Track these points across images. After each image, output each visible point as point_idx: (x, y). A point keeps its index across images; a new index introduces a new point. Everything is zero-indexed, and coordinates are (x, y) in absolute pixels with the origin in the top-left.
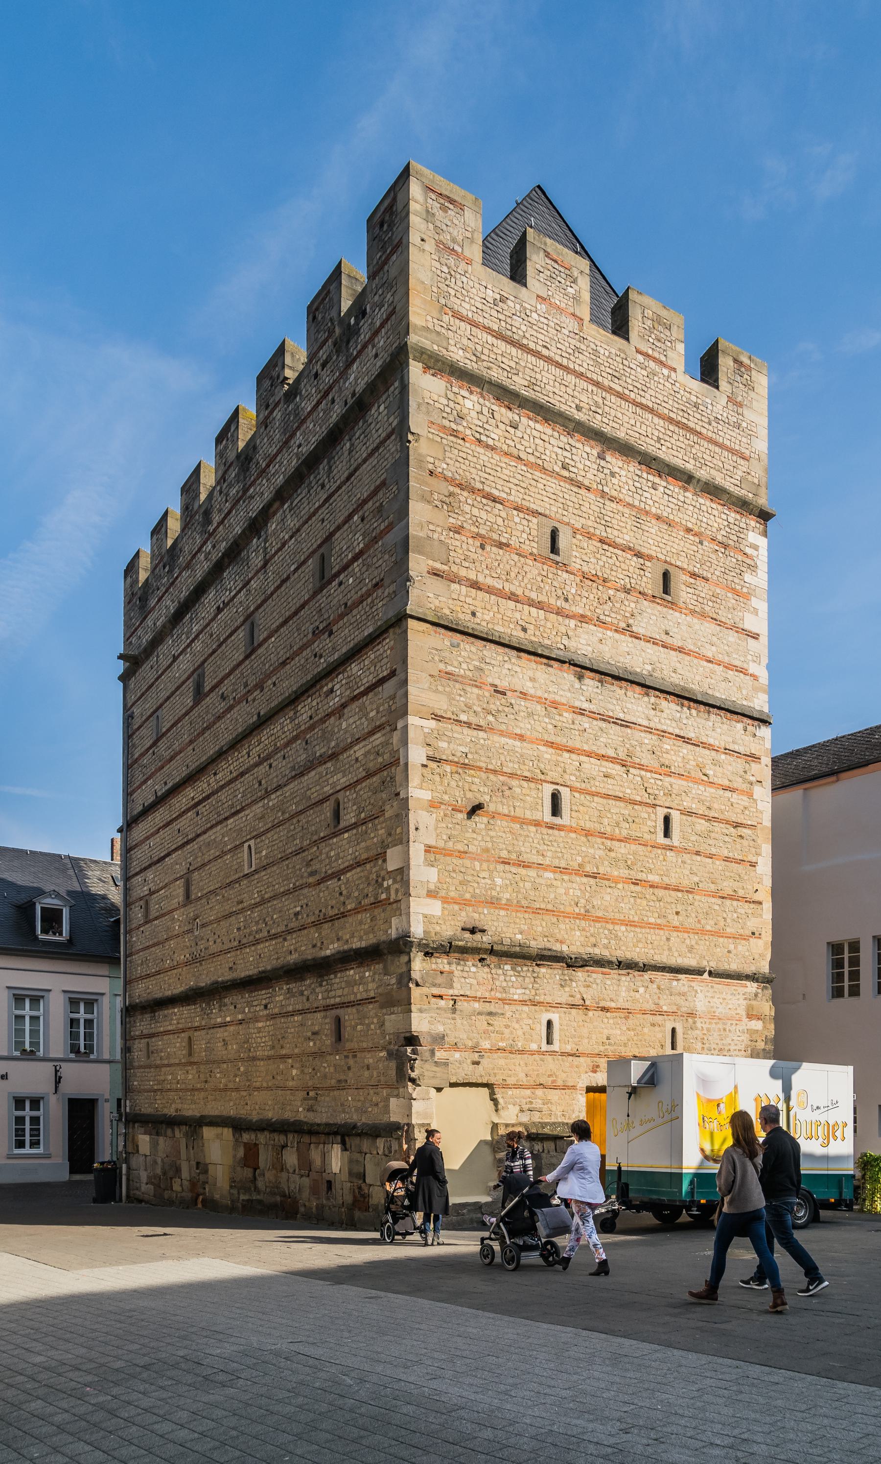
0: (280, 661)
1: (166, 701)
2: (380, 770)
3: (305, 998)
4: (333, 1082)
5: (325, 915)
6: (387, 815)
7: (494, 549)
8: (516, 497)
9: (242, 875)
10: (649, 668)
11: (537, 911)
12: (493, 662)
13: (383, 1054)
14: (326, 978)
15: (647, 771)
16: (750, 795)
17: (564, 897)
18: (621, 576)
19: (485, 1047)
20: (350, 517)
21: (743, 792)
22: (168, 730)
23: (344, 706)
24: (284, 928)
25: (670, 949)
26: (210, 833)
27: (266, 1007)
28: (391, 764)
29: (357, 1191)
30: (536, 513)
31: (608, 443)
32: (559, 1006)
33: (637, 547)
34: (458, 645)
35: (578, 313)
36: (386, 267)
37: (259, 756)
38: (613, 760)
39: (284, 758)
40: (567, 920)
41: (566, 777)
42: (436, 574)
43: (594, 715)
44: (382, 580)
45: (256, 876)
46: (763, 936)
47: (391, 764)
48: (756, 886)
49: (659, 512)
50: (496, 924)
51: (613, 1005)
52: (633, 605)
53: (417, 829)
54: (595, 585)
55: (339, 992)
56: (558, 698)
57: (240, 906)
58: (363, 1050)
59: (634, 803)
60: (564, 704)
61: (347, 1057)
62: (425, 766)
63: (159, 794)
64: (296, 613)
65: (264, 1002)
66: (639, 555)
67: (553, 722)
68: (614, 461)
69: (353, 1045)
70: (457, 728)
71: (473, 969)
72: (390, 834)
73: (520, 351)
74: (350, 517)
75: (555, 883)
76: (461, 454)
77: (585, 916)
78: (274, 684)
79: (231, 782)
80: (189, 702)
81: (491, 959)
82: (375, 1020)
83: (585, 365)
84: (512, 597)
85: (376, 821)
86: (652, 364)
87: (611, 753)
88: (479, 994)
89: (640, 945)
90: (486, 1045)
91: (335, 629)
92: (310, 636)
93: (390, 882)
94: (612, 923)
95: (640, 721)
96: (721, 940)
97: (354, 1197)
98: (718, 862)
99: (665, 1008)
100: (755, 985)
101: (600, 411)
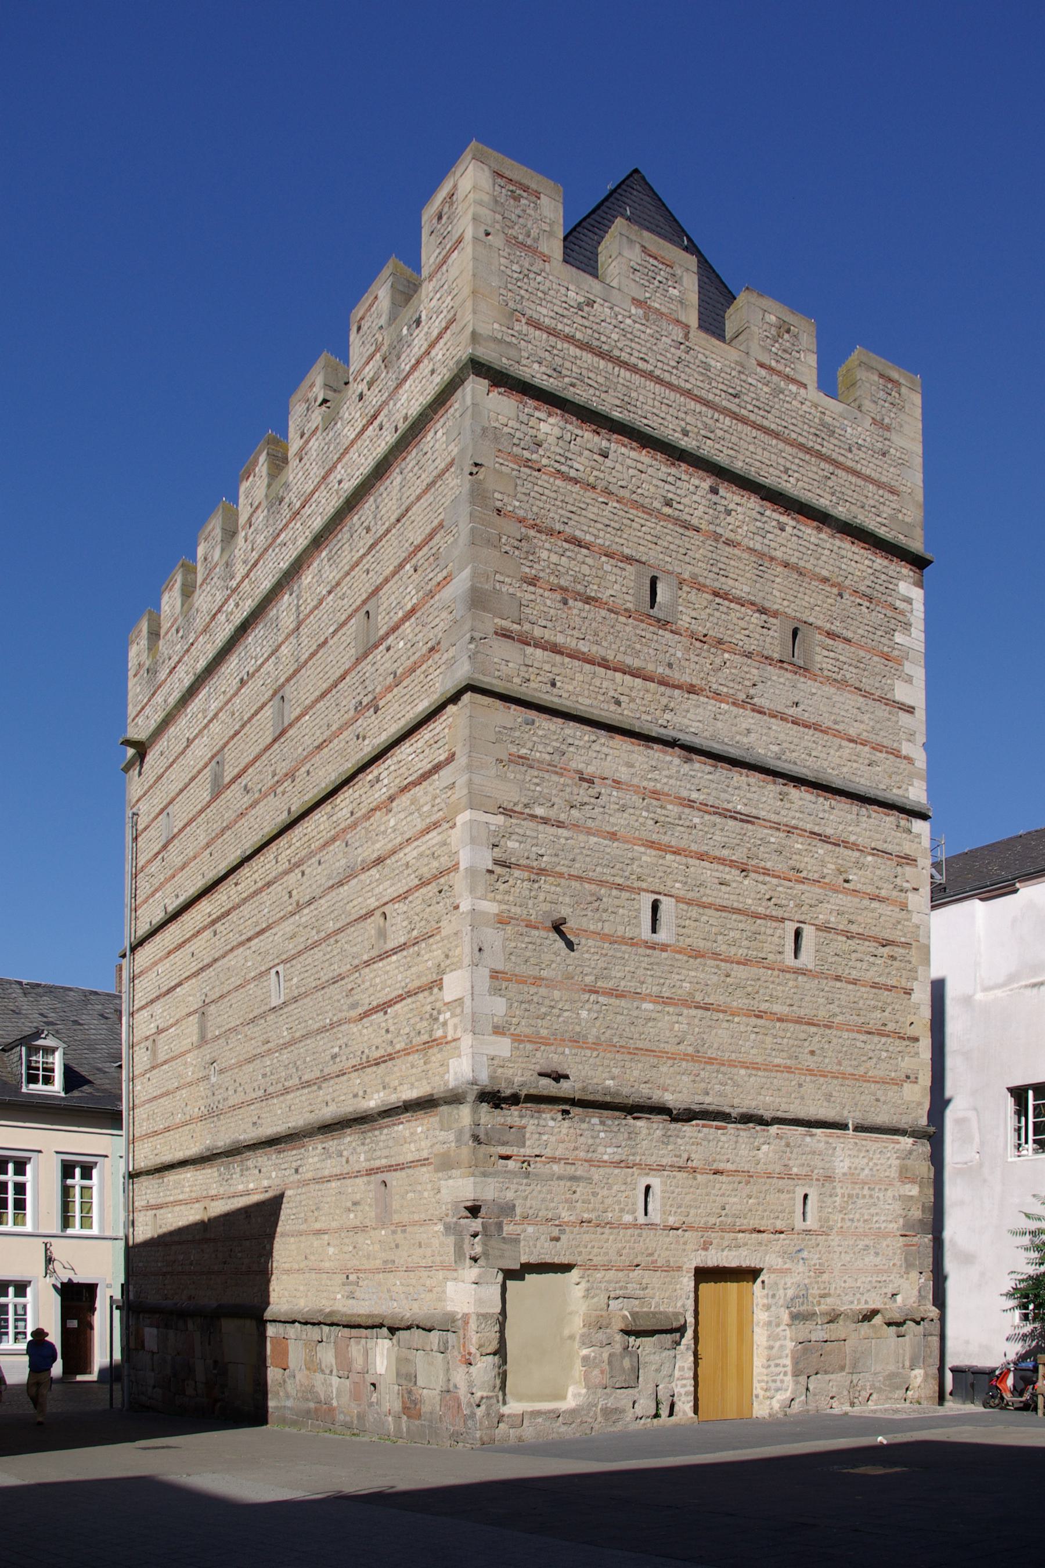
0: (316, 744)
1: (178, 795)
2: (436, 877)
3: (344, 1160)
4: (378, 1263)
5: (368, 1057)
6: (444, 933)
7: (580, 604)
8: (605, 539)
9: (268, 1008)
10: (775, 748)
11: (635, 1052)
12: (576, 743)
13: (440, 1227)
14: (370, 1134)
15: (774, 876)
16: (904, 907)
17: (668, 1034)
18: (738, 636)
19: (566, 1220)
20: (401, 566)
21: (894, 902)
22: (181, 831)
23: (392, 799)
24: (318, 1074)
25: (802, 1098)
26: (230, 956)
27: (297, 1171)
28: (448, 871)
29: (406, 1395)
30: (629, 559)
31: (722, 474)
32: (662, 1168)
33: (758, 601)
34: (533, 723)
35: (683, 319)
36: (444, 268)
37: (289, 861)
38: (732, 864)
39: (320, 863)
40: (670, 1062)
41: (669, 883)
42: (505, 634)
43: (705, 808)
44: (439, 643)
45: (285, 1010)
46: (919, 1080)
47: (448, 871)
48: (911, 1018)
49: (786, 557)
50: (580, 1067)
51: (729, 1166)
52: (755, 671)
53: (480, 950)
54: (706, 647)
55: (385, 1152)
56: (659, 786)
57: (266, 1047)
58: (414, 1223)
59: (757, 916)
60: (668, 795)
61: (394, 1232)
62: (491, 872)
63: (170, 909)
64: (335, 685)
65: (294, 1165)
66: (763, 611)
67: (652, 815)
68: (730, 496)
69: (405, 1218)
70: (532, 824)
71: (551, 1123)
72: (447, 956)
73: (610, 365)
74: (401, 566)
75: (654, 1015)
76: (536, 488)
77: (693, 1058)
78: (308, 773)
79: (256, 893)
80: (206, 796)
81: (575, 1111)
82: (429, 1186)
83: (692, 380)
84: (605, 664)
85: (431, 940)
86: (775, 378)
87: (725, 853)
88: (557, 1154)
89: (763, 1092)
90: (566, 1215)
91: (381, 703)
92: (352, 713)
93: (448, 1015)
94: (730, 1065)
95: (762, 814)
96: (865, 1084)
97: (403, 1402)
98: (863, 989)
99: (795, 1170)
100: (911, 1140)
101: (712, 436)
